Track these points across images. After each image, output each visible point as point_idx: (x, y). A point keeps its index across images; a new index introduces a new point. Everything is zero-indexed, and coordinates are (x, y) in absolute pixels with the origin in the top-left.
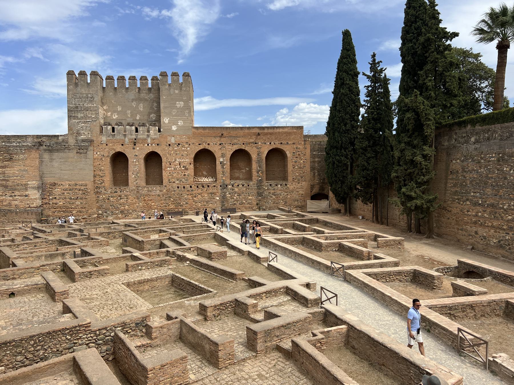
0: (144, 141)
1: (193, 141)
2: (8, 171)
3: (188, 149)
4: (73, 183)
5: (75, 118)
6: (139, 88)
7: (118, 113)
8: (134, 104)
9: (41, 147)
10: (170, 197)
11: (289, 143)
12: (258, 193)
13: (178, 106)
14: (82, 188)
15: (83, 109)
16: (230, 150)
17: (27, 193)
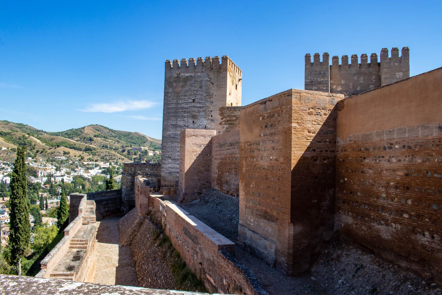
6: (360, 64)
8: (355, 78)
13: (398, 76)
15: (316, 83)
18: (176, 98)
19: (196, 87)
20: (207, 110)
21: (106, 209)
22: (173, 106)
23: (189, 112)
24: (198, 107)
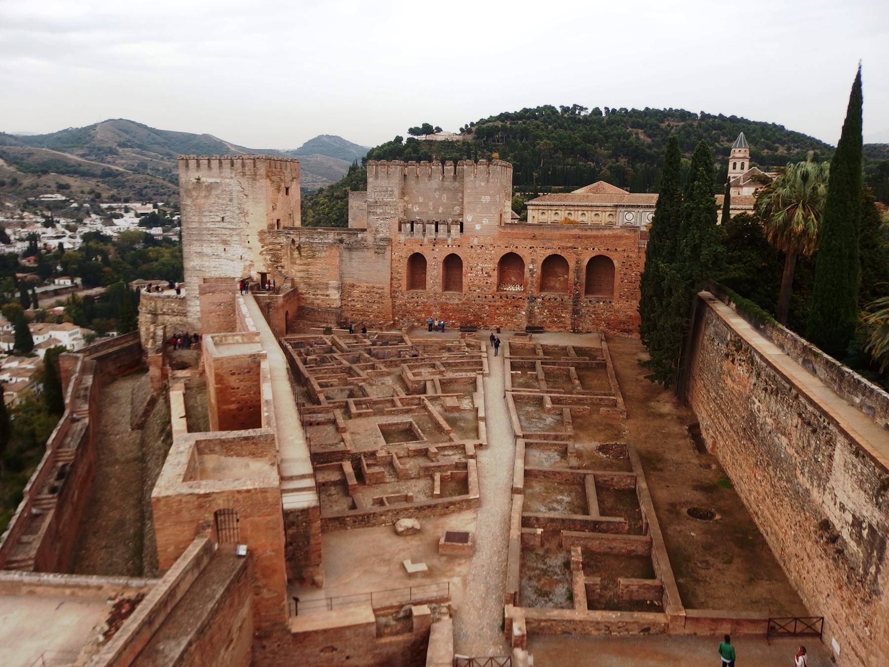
0: (445, 241)
1: (499, 243)
2: (311, 268)
3: (493, 252)
4: (371, 285)
5: (375, 213)
7: (420, 204)
8: (437, 194)
9: (341, 245)
10: (470, 307)
11: (618, 249)
12: (573, 310)
13: (484, 201)
14: (380, 291)
16: (542, 255)
17: (328, 293)
18: (198, 214)
19: (224, 199)
20: (242, 233)
21: (118, 365)
22: (194, 225)
23: (217, 235)
24: (230, 229)
